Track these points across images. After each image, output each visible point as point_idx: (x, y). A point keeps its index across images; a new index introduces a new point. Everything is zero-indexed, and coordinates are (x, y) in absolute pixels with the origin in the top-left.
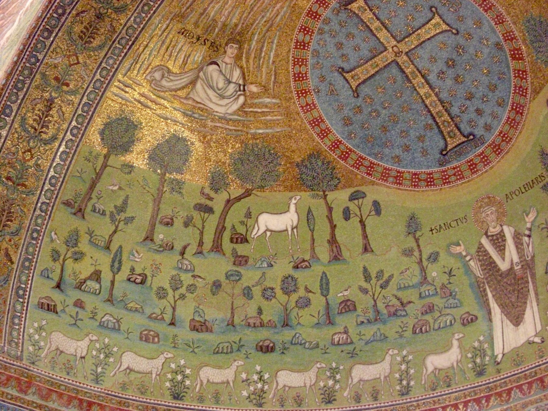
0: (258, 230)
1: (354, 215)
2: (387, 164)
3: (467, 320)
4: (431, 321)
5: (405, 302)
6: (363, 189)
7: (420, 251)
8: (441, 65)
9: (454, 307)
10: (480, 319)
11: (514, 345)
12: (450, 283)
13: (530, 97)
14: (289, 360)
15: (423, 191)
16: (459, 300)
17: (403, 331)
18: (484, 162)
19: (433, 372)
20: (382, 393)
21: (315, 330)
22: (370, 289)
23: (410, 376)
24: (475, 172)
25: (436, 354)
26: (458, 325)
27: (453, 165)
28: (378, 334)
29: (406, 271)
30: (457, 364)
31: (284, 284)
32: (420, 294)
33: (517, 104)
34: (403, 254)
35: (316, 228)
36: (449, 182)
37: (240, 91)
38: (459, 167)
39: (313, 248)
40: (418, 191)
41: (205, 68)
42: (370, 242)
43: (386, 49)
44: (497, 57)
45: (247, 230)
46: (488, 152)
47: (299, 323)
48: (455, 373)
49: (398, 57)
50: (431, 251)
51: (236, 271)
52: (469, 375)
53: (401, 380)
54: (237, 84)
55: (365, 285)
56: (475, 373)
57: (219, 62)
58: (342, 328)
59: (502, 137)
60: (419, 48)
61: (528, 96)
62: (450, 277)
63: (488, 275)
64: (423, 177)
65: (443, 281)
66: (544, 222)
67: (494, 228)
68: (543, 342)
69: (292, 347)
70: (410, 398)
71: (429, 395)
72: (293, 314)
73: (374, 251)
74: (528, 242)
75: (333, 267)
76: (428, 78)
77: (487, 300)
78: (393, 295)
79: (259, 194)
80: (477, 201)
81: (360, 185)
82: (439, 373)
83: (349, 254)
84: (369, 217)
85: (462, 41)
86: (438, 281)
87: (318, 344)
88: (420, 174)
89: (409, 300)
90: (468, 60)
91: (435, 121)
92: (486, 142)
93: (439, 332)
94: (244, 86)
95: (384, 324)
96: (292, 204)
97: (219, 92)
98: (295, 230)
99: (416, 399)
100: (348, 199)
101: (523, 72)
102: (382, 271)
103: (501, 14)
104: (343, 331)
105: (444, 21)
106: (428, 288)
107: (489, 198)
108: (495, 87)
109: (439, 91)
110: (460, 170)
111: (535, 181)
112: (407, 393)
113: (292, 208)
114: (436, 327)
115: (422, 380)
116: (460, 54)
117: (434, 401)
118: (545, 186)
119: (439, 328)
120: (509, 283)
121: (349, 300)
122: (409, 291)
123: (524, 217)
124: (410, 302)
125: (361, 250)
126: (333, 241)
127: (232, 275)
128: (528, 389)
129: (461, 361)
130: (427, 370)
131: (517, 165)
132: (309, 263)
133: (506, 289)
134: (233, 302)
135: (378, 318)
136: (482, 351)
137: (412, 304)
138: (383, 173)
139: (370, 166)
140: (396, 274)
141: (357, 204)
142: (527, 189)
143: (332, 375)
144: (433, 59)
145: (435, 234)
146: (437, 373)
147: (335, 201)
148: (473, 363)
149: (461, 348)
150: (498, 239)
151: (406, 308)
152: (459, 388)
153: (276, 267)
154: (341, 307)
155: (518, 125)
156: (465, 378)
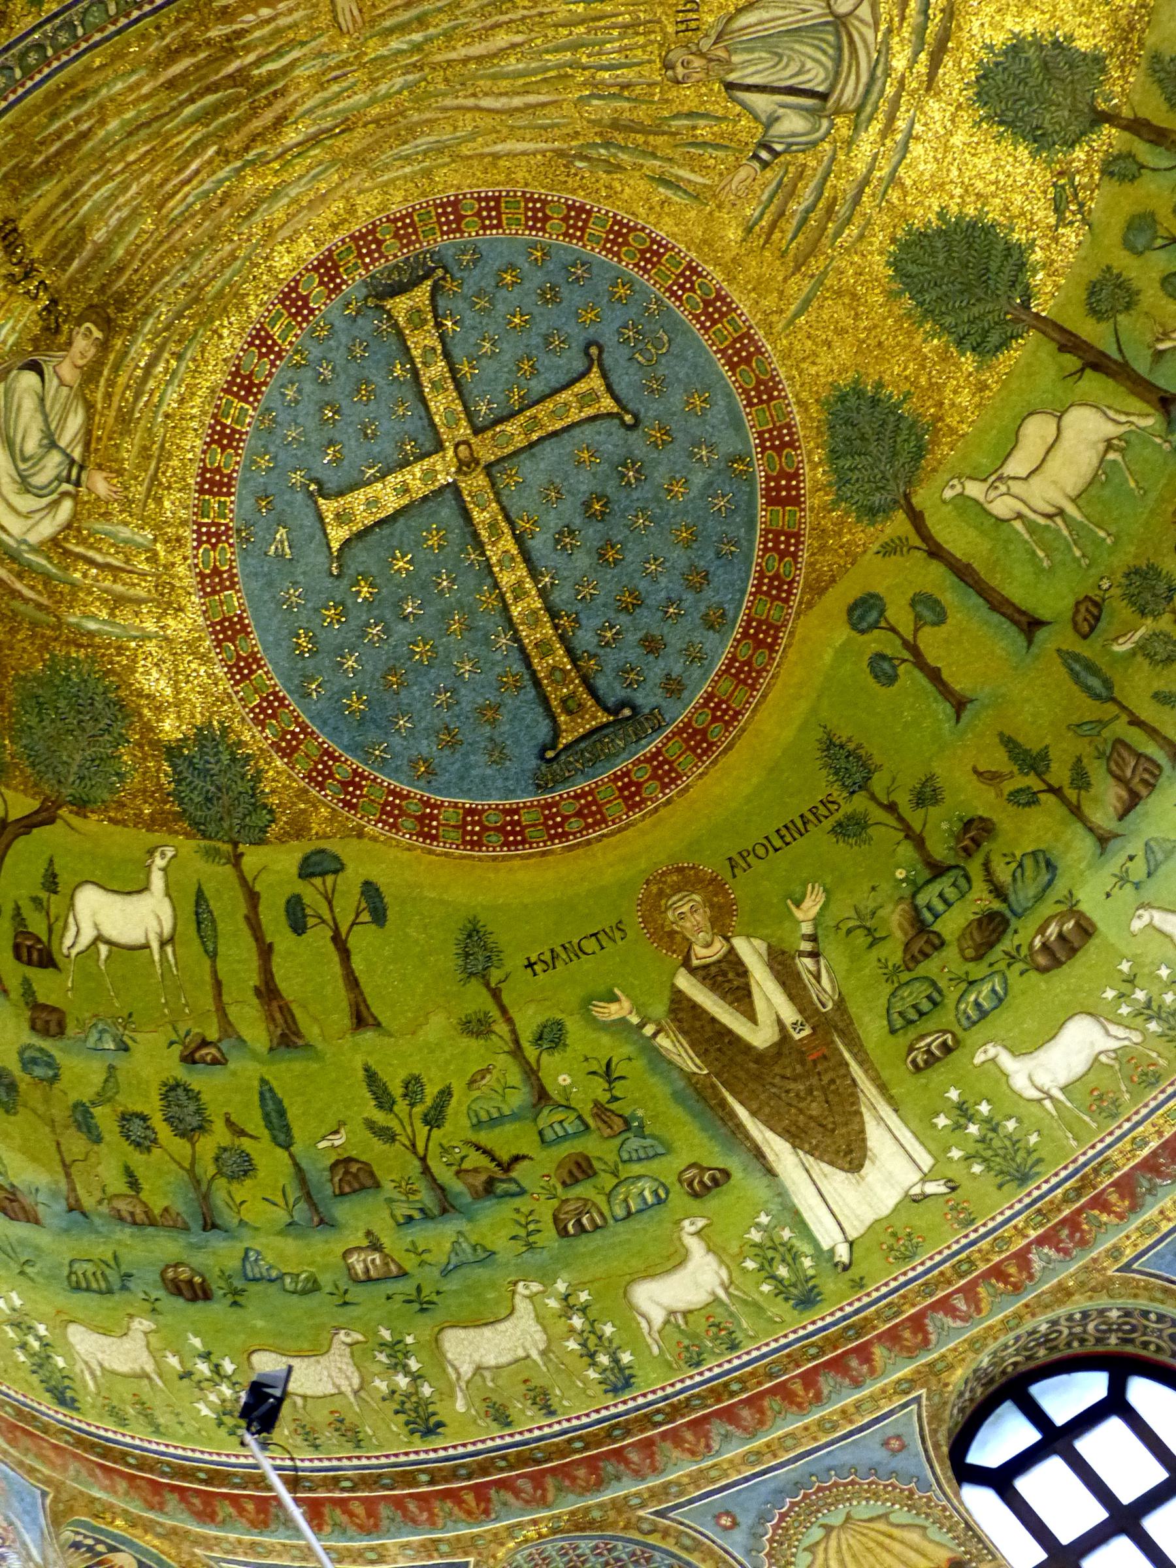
0: (78, 932)
1: (317, 920)
2: (397, 780)
3: (701, 1182)
4: (601, 1200)
6: (333, 846)
7: (509, 1021)
8: (570, 511)
9: (648, 1158)
10: (737, 1174)
11: (870, 1217)
12: (615, 1099)
13: (800, 603)
14: (260, 1324)
15: (495, 859)
17: (529, 1234)
18: (660, 779)
19: (667, 1322)
20: (558, 1392)
21: (290, 1240)
22: (398, 1129)
23: (610, 1341)
24: (637, 805)
26: (679, 1198)
27: (577, 788)
28: (464, 1245)
29: (483, 1078)
30: (726, 1289)
31: (168, 1106)
32: (541, 1133)
33: (760, 623)
35: (221, 949)
36: (565, 834)
37: (68, 481)
38: (591, 792)
39: (221, 1011)
40: (480, 859)
41: (15, 372)
43: (439, 447)
44: (724, 496)
45: (50, 931)
46: (674, 747)
47: (242, 1223)
48: (732, 1314)
49: (465, 474)
50: (540, 1019)
51: (41, 1050)
52: (775, 1310)
53: (592, 1355)
54: (67, 455)
55: (380, 1117)
56: (792, 1302)
57: (48, 370)
58: (361, 1234)
59: (714, 710)
60: (523, 456)
61: (794, 602)
62: (610, 1082)
64: (493, 819)
65: (593, 1096)
66: (853, 914)
67: (708, 945)
68: (953, 1189)
69: (254, 1288)
71: (691, 1377)
72: (220, 1196)
74: (813, 968)
75: (283, 1066)
76: (531, 543)
77: (740, 1126)
78: (467, 1143)
79: (75, 821)
80: (647, 882)
81: (326, 837)
82: (686, 1323)
83: (316, 1030)
84: (355, 928)
85: (641, 449)
86: (581, 1096)
87: (315, 1281)
88: (484, 811)
89: (514, 1152)
90: (646, 500)
91: (529, 665)
92: (668, 725)
93: (633, 1224)
94: (82, 468)
95: (470, 1220)
96: (154, 869)
97: (22, 466)
98: (169, 949)
99: (660, 1394)
100: (294, 870)
101: (789, 536)
102: (417, 1079)
103: (773, 378)
104: (365, 1243)
105: (609, 388)
106: (561, 1117)
107: (680, 870)
108: (706, 577)
109: (552, 584)
110: (594, 802)
111: (811, 817)
112: (627, 1383)
113: (157, 881)
114: (620, 1212)
116: (629, 484)
119: (629, 1214)
121: (349, 1160)
122: (509, 1128)
124: (517, 1159)
126: (268, 992)
127: (34, 1061)
128: (1020, 1271)
129: (731, 1283)
130: (649, 1323)
131: (755, 780)
132: (219, 1049)
134: (58, 1144)
135: (446, 1206)
136: (781, 1249)
137: (526, 1163)
138: (387, 803)
139: (352, 783)
140: (458, 1087)
141: (321, 888)
143: (394, 1361)
144: (553, 492)
147: (263, 875)
149: (715, 1253)
150: (725, 974)
153: (139, 1053)
154: (337, 1179)
155: (759, 676)
156: (771, 1320)
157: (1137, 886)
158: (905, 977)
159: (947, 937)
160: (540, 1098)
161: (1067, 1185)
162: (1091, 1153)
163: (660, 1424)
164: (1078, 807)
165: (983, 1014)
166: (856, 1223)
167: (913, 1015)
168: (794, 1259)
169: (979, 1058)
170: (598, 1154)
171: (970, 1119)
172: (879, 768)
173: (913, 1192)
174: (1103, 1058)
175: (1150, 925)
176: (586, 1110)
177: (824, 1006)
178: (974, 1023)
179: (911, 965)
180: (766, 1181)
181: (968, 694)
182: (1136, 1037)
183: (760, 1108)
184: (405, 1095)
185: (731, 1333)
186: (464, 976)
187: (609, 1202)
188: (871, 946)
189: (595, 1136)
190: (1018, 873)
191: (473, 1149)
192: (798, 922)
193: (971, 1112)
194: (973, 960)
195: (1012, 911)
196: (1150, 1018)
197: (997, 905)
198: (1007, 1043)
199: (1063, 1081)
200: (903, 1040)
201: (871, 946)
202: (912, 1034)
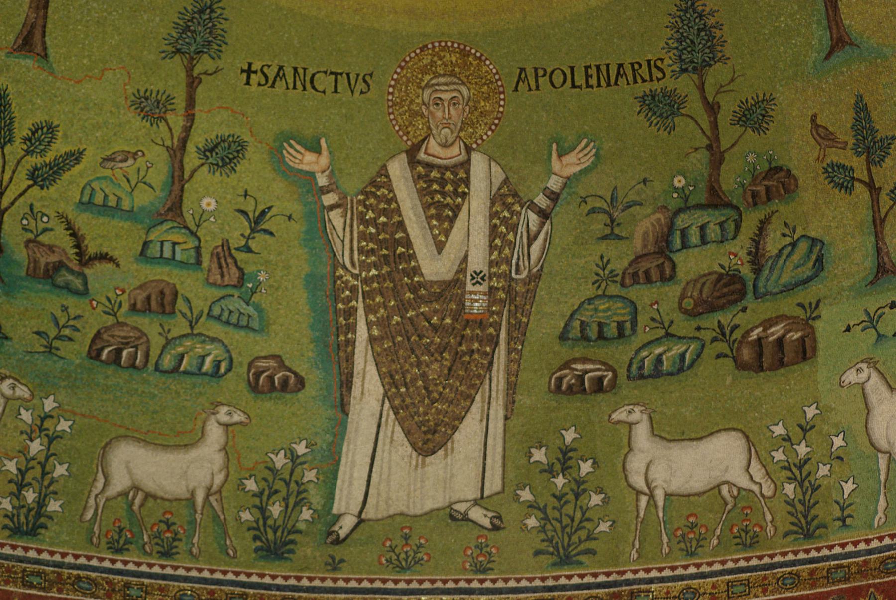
3: (271, 378)
4: (157, 342)
5: (92, 249)
7: (190, 117)
9: (237, 326)
10: (310, 391)
12: (249, 250)
16: (258, 308)
19: (124, 494)
25: (147, 443)
29: (126, 160)
32: (146, 245)
34: (133, 103)
42: (49, 26)
48: (193, 522)
50: (225, 131)
53: (21, 486)
56: (259, 543)
62: (253, 230)
63: (374, 272)
65: (226, 236)
67: (445, 146)
68: (495, 528)
70: (40, 551)
71: (101, 559)
73: (51, 59)
74: (533, 228)
77: (352, 343)
78: (61, 216)
82: (142, 506)
89: (104, 250)
99: (57, 558)
102: (51, 129)
107: (465, 54)
111: (629, 72)
112: (33, 532)
114: (167, 362)
115: (85, 508)
117: (110, 583)
118: (653, 97)
119: (175, 370)
120: (435, 320)
123: (550, 155)
124: (103, 257)
125: (12, 38)
129: (219, 491)
130: (106, 485)
133: (420, 337)
137: (110, 266)
142: (593, 81)
145: (254, 87)
146: (138, 502)
148: (258, 514)
150: (442, 182)
151: (87, 271)
152: (200, 570)
157: (880, 336)
158: (614, 289)
159: (681, 274)
160: (170, 209)
161: (595, 592)
162: (641, 575)
163: (32, 586)
164: (883, 221)
165: (657, 373)
166: (382, 505)
167: (593, 333)
168: (296, 504)
169: (620, 415)
170: (189, 295)
171: (565, 469)
172: (724, 59)
173: (456, 507)
174: (725, 490)
175: (862, 386)
176: (210, 244)
177: (518, 271)
178: (642, 377)
179: (627, 281)
180: (330, 413)
181: (854, 35)
182: (767, 491)
183: (381, 338)
184: (27, 140)
185: (174, 540)
186: (170, 49)
187: (164, 347)
188: (605, 237)
189: (201, 276)
190: (786, 252)
191: (63, 226)
192: (550, 172)
193: (570, 463)
194: (686, 312)
195: (754, 286)
196: (792, 479)
197: (746, 271)
198: (656, 417)
199: (673, 488)
200: (566, 352)
201: (605, 237)
202: (578, 352)
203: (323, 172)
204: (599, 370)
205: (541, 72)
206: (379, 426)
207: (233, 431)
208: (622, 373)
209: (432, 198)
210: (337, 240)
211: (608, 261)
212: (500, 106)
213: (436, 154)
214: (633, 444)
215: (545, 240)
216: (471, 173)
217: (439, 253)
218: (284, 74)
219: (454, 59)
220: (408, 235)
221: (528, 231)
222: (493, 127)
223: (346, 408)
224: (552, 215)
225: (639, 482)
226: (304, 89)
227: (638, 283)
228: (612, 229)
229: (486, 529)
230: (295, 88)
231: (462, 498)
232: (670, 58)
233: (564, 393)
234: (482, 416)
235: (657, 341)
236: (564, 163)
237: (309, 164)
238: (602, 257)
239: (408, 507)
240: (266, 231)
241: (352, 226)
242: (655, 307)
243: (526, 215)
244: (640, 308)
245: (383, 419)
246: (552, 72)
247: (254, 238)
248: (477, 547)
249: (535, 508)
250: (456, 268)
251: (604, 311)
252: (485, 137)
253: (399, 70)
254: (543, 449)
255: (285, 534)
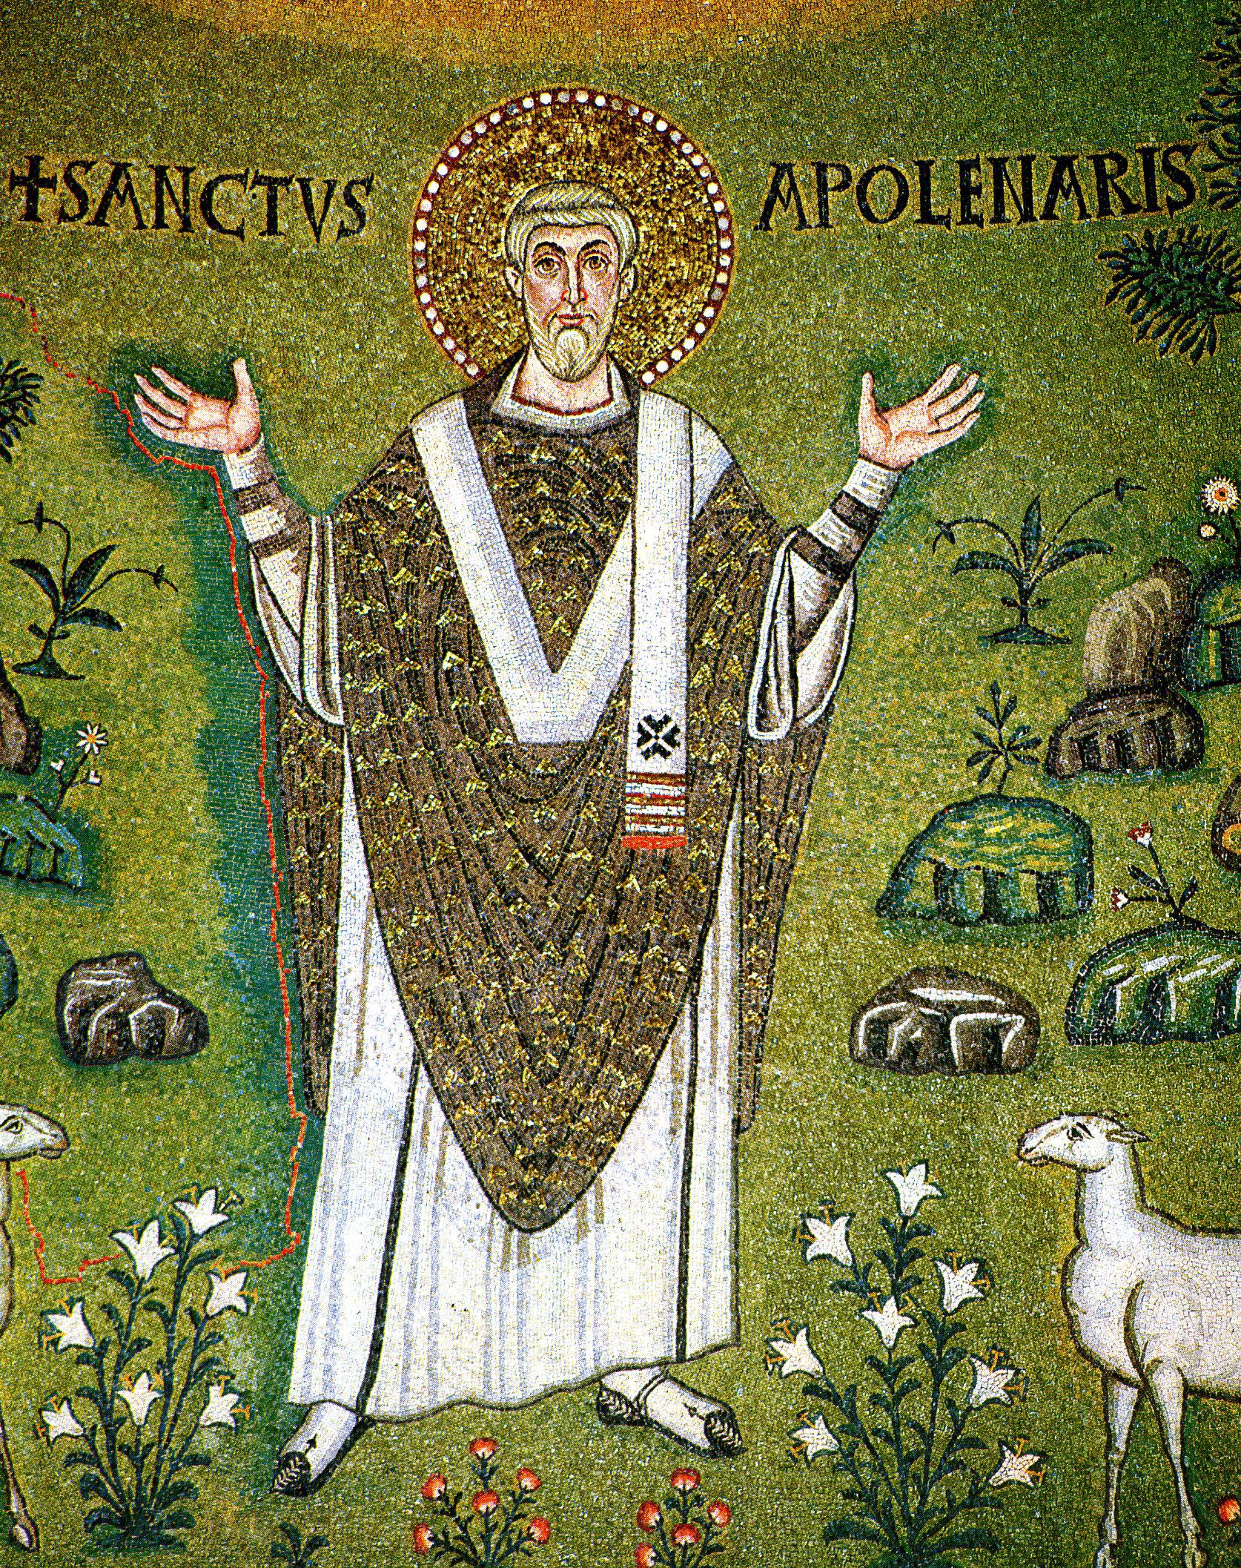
3: (120, 1020)
12: (53, 670)
56: (96, 1503)
67: (568, 377)
68: (720, 1449)
74: (806, 606)
123: (854, 406)
136: (184, 1328)
148: (91, 1413)
166: (419, 1378)
168: (193, 1378)
173: (613, 1382)
178: (1110, 1035)
179: (1064, 760)
188: (998, 638)
199: (1208, 1372)
203: (244, 450)
204: (985, 1006)
205: (834, 176)
206: (404, 1150)
207: (22, 1175)
208: (1052, 1016)
209: (535, 520)
210: (284, 634)
211: (1013, 702)
212: (719, 269)
213: (544, 398)
214: (1088, 1229)
215: (838, 635)
216: (641, 449)
217: (554, 670)
218: (129, 187)
219: (594, 140)
220: (471, 617)
221: (791, 611)
222: (700, 328)
223: (319, 1097)
224: (858, 569)
225: (1109, 1345)
226: (186, 225)
227: (1095, 767)
228: (1024, 614)
229: (696, 1449)
230: (160, 223)
231: (627, 1360)
232: (1213, 147)
233: (894, 1067)
234: (676, 1121)
235: (1148, 936)
236: (895, 427)
237: (206, 428)
238: (994, 690)
239: (487, 1385)
240: (92, 615)
241: (322, 597)
242: (1145, 839)
243: (787, 567)
244: (1100, 841)
245: (416, 1127)
246: (867, 178)
247: (66, 635)
248: (672, 1503)
249: (827, 1395)
250: (599, 708)
251: (999, 839)
252: (676, 355)
253: (443, 170)
254: (842, 1221)
255: (166, 1466)
